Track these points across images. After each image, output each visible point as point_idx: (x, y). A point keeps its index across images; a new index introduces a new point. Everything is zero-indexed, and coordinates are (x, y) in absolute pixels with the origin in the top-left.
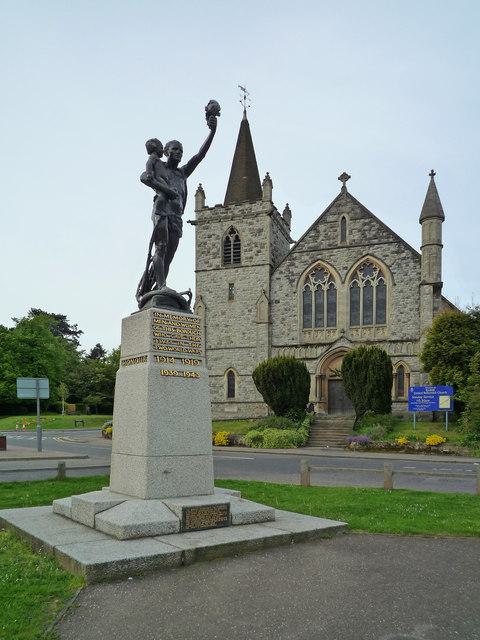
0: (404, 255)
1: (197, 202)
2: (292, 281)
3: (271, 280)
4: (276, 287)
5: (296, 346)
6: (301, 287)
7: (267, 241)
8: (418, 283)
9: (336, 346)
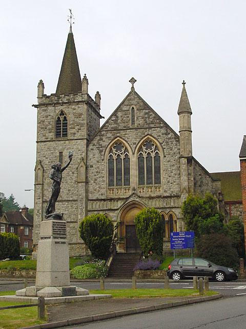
0: (170, 136)
1: (38, 92)
2: (101, 151)
3: (87, 150)
4: (91, 156)
5: (104, 200)
6: (107, 156)
7: (85, 122)
8: (178, 156)
9: (130, 200)
